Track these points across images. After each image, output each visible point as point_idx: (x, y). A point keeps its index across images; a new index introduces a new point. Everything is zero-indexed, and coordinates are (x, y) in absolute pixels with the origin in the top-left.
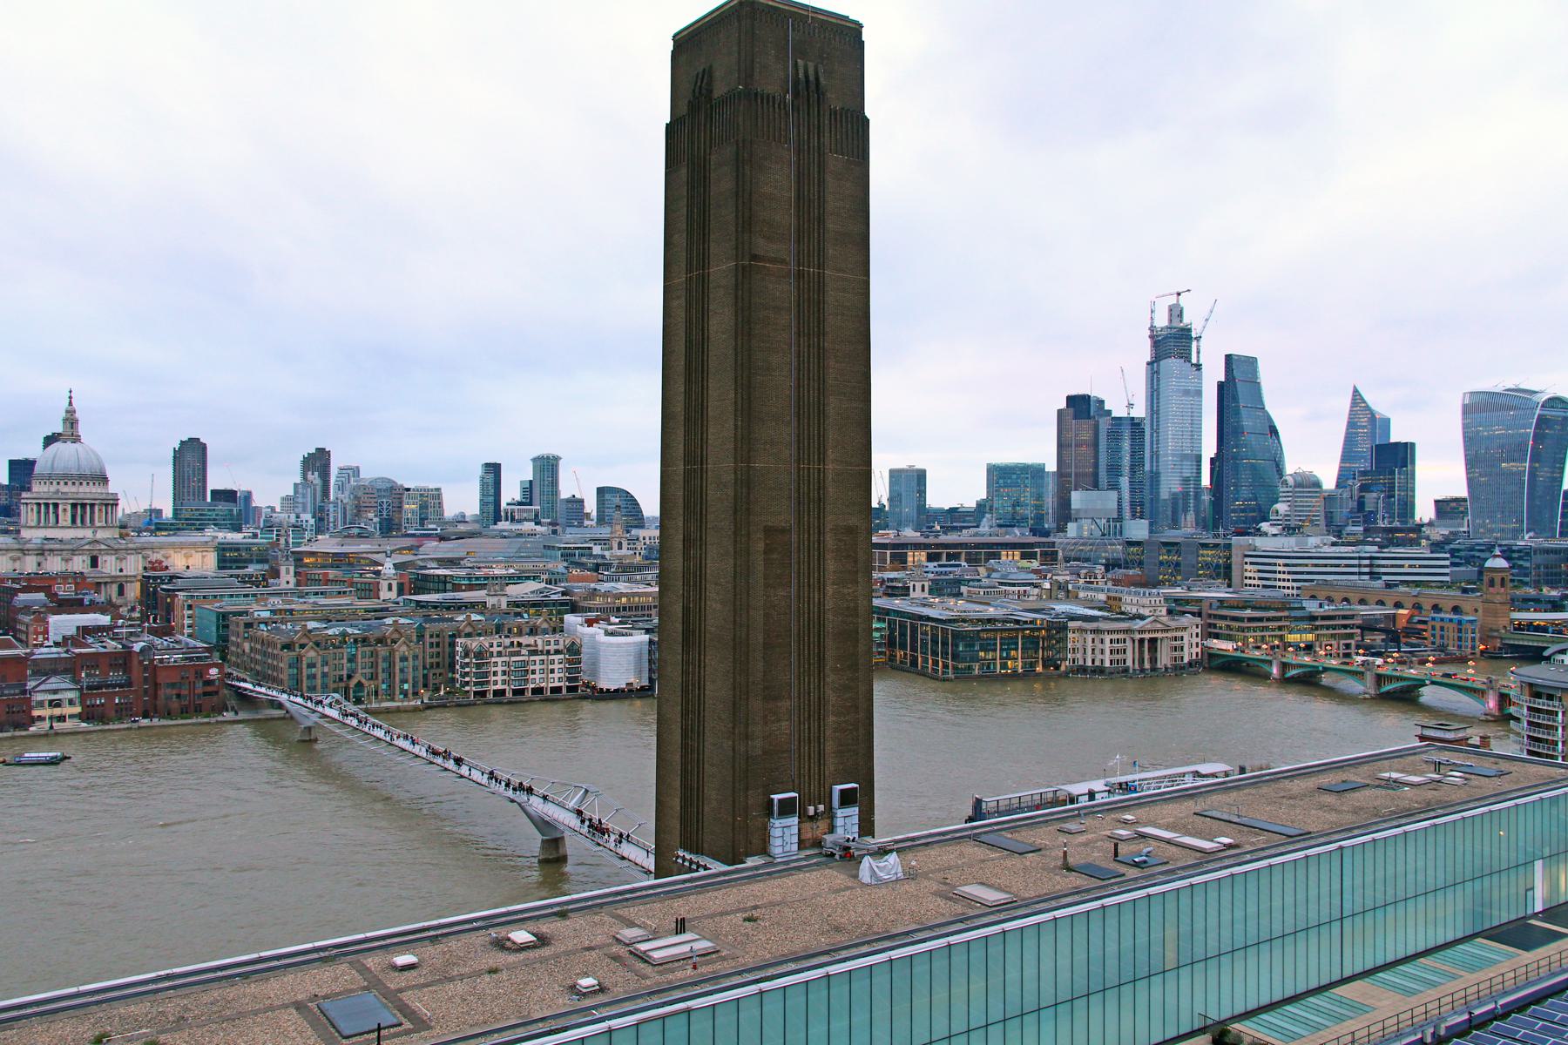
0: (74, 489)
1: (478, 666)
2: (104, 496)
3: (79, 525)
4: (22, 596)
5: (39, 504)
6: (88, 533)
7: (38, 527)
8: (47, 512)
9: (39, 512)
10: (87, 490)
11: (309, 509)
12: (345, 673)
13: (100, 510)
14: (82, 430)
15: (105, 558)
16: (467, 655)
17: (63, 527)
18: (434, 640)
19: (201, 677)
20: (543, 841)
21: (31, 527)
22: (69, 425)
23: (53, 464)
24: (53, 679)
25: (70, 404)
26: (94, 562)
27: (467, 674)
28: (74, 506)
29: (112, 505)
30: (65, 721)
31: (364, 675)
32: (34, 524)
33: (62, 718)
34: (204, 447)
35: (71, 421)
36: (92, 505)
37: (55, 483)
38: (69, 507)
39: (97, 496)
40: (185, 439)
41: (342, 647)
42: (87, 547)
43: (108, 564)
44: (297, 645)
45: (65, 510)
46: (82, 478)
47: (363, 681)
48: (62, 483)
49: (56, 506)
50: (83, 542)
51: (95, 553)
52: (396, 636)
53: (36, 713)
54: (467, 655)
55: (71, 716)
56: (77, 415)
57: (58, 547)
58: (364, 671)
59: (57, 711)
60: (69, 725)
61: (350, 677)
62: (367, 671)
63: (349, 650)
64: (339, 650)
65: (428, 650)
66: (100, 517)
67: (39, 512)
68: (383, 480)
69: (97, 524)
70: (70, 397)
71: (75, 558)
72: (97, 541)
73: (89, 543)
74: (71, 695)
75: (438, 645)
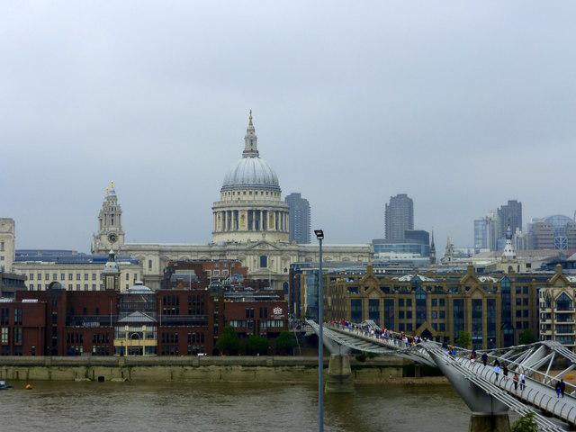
0: (251, 198)
1: (562, 317)
2: (274, 204)
3: (254, 229)
4: (179, 273)
5: (224, 212)
6: (256, 237)
7: (223, 232)
8: (229, 223)
9: (224, 220)
10: (262, 198)
11: (488, 244)
12: (413, 321)
13: (271, 217)
14: (260, 146)
15: (274, 258)
16: (549, 304)
17: (241, 232)
18: (522, 296)
19: (266, 317)
20: (474, 419)
21: (219, 233)
22: (249, 143)
23: (235, 176)
24: (137, 313)
25: (251, 124)
26: (263, 263)
27: (549, 327)
28: (250, 212)
29: (282, 212)
30: (141, 354)
31: (435, 326)
32: (220, 230)
33: (138, 351)
34: (410, 202)
35: (251, 139)
36: (265, 212)
37: (236, 193)
38: (246, 214)
39: (268, 204)
40: (395, 195)
41: (410, 293)
42: (257, 248)
43: (275, 264)
44: (362, 288)
45: (243, 216)
46: (257, 187)
47: (431, 330)
48: (242, 193)
49: (236, 212)
50: (254, 244)
51: (264, 254)
52: (468, 284)
53: (117, 343)
54: (549, 304)
55: (149, 349)
56: (256, 133)
57: (233, 247)
58: (434, 321)
59: (135, 343)
60: (146, 357)
61: (418, 326)
62: (439, 321)
63: (419, 297)
64: (408, 296)
65: (514, 308)
66: (271, 224)
67: (224, 220)
68: (559, 218)
69: (269, 229)
70: (251, 118)
71: (248, 257)
72: (264, 243)
73: (259, 244)
74: (150, 329)
75: (526, 301)
